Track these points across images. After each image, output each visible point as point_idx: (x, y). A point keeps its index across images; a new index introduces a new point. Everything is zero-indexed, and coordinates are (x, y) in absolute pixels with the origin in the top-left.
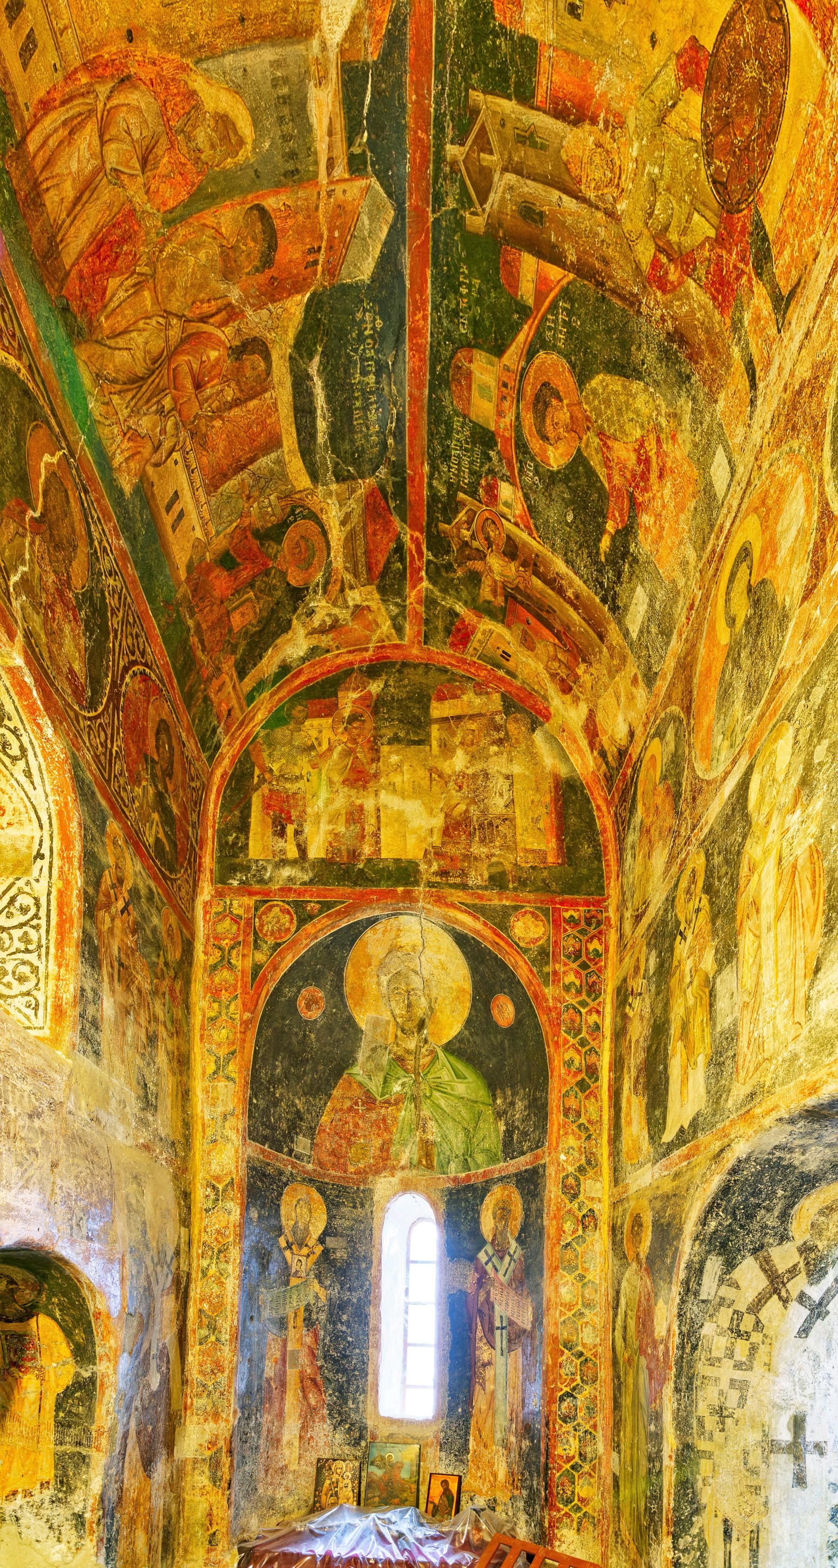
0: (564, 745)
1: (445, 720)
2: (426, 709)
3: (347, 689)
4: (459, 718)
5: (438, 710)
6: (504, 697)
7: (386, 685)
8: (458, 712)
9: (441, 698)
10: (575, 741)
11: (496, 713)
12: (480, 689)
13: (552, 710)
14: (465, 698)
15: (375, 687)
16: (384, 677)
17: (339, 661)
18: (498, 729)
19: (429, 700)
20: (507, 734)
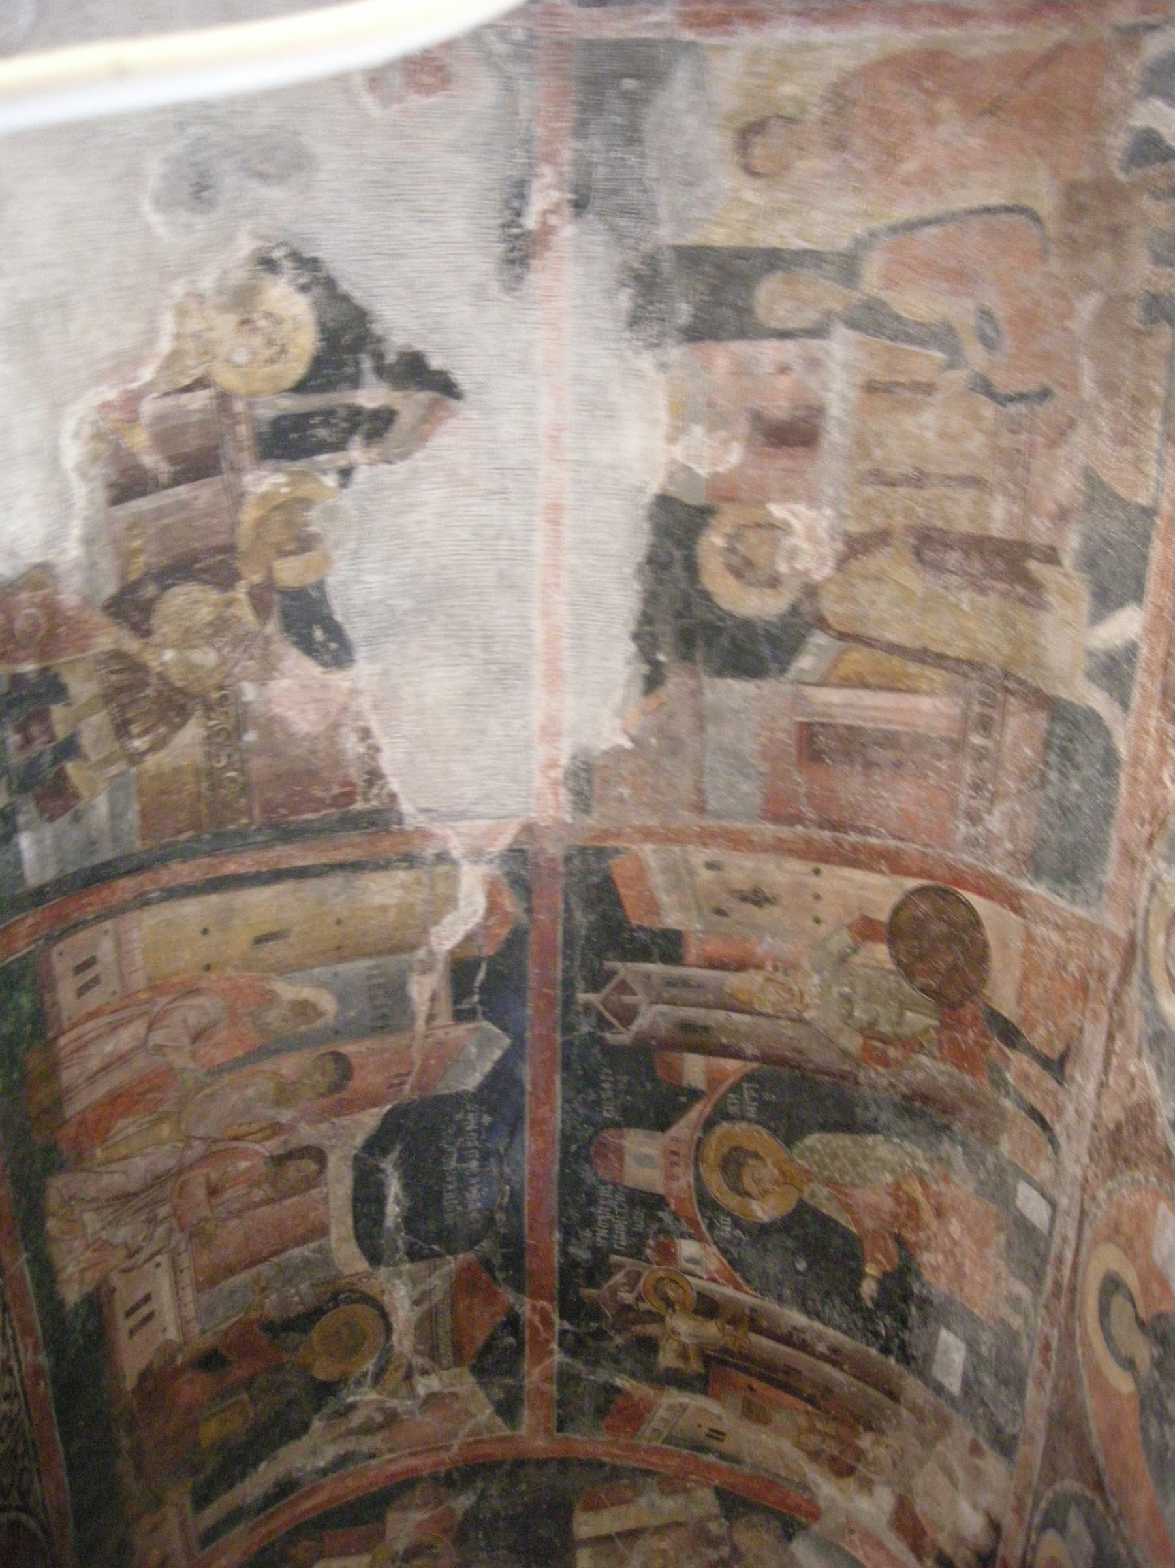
0: (859, 1555)
1: (600, 1541)
2: (565, 1527)
3: (405, 1508)
4: (631, 1535)
5: (586, 1525)
6: (719, 1492)
7: (483, 1496)
8: (631, 1524)
9: (594, 1506)
10: (879, 1545)
11: (709, 1518)
12: (671, 1485)
13: (822, 1504)
14: (643, 1501)
15: (463, 1502)
16: (480, 1485)
17: (392, 1468)
18: (714, 1543)
19: (570, 1511)
20: (735, 1549)
